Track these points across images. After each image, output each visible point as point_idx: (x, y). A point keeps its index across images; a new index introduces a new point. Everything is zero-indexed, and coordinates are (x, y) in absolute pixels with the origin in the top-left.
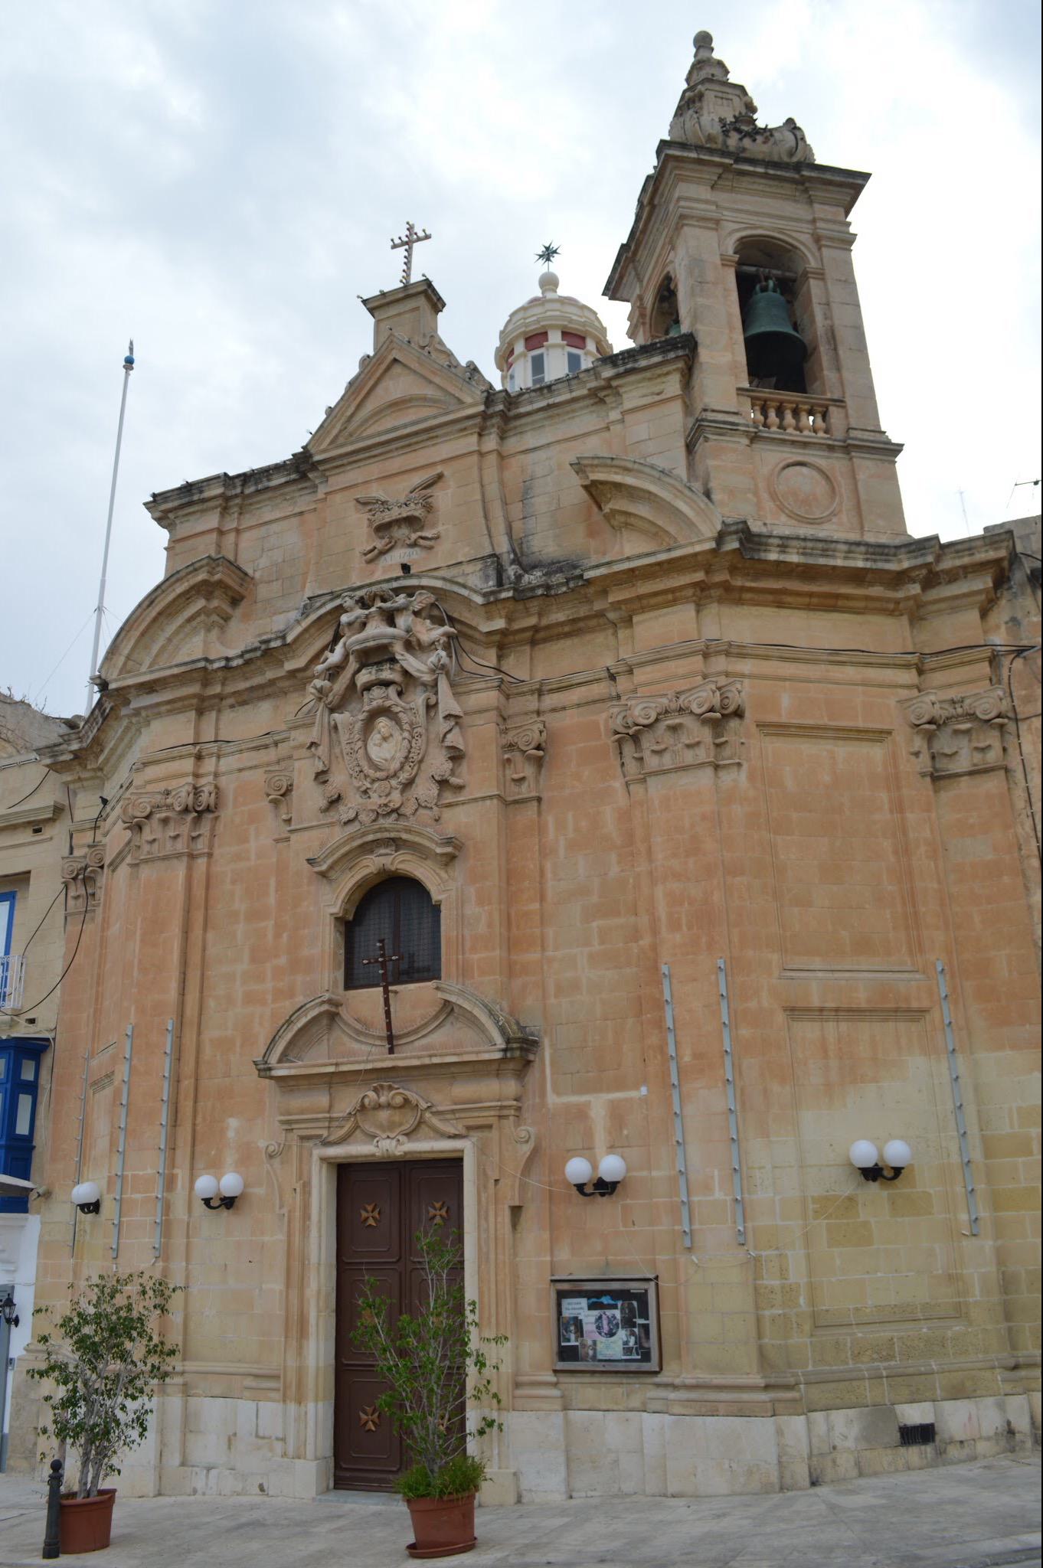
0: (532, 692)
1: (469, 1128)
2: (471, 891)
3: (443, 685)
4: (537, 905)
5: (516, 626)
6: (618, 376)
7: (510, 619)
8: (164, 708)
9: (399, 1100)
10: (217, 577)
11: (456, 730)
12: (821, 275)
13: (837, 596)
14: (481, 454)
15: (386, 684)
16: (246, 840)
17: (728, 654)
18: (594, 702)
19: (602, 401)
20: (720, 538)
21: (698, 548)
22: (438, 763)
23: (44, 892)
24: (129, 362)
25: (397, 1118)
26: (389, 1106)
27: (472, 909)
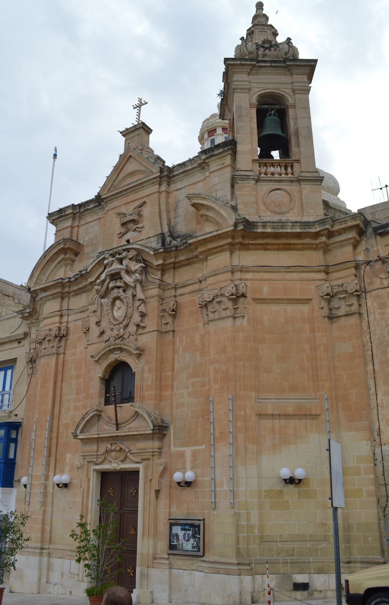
0: (173, 288)
1: (142, 459)
2: (146, 368)
3: (138, 287)
4: (170, 373)
5: (167, 262)
6: (207, 158)
7: (165, 260)
8: (50, 297)
9: (118, 448)
10: (67, 246)
11: (143, 305)
12: (294, 106)
13: (290, 244)
14: (160, 192)
15: (119, 287)
16: (76, 348)
17: (241, 271)
18: (194, 292)
19: (203, 168)
20: (236, 225)
21: (227, 230)
22: (136, 318)
23: (21, 365)
24: (55, 156)
25: (118, 455)
26: (115, 450)
27: (146, 375)
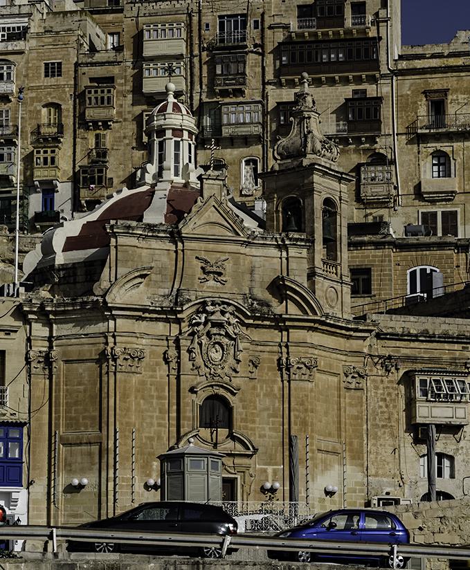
6: (290, 244)
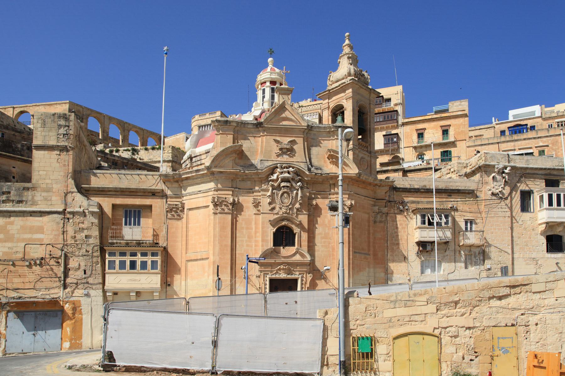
22: (297, 206)
